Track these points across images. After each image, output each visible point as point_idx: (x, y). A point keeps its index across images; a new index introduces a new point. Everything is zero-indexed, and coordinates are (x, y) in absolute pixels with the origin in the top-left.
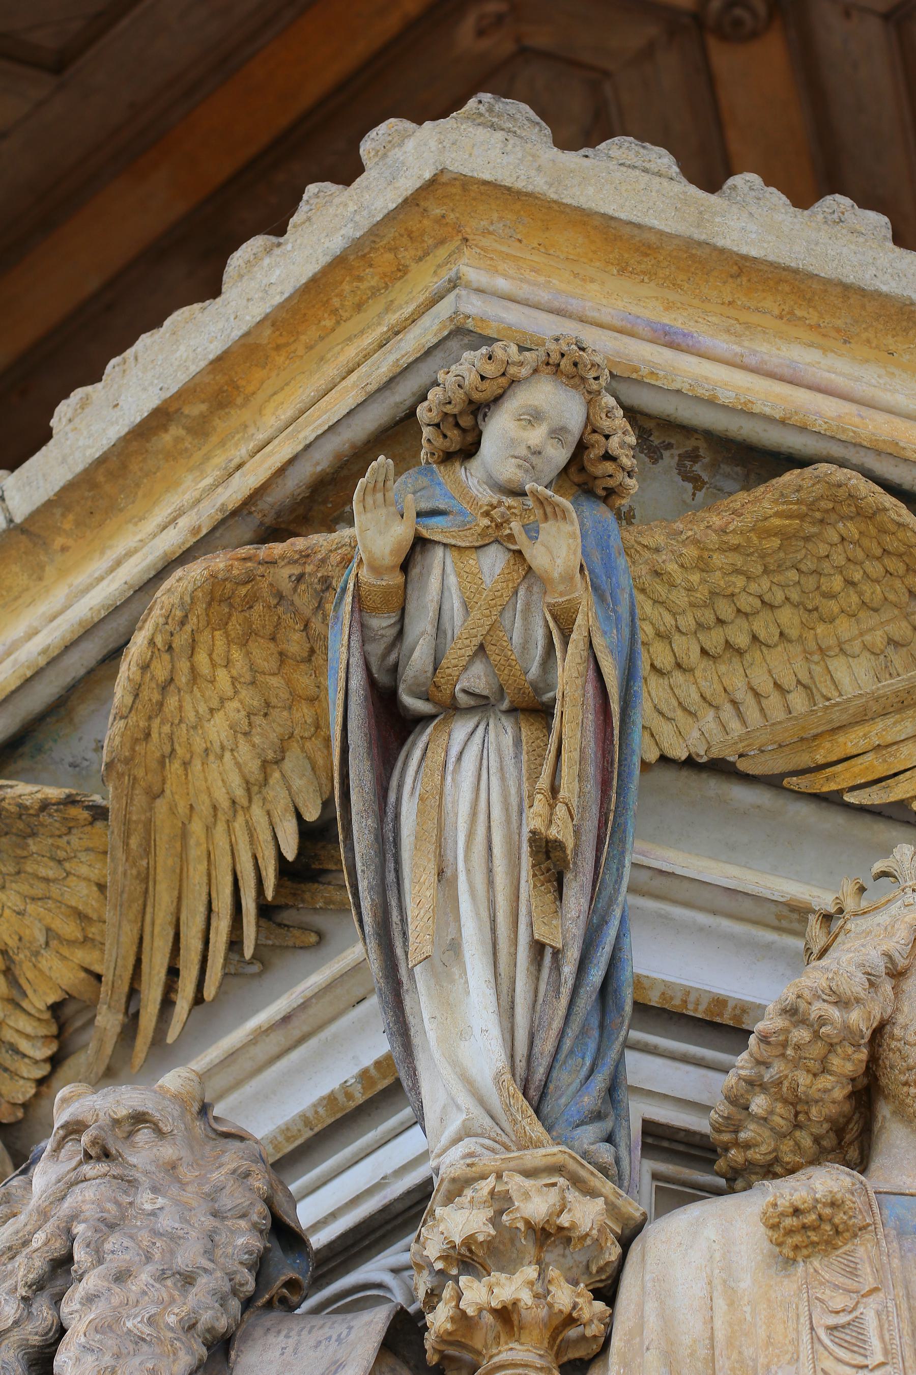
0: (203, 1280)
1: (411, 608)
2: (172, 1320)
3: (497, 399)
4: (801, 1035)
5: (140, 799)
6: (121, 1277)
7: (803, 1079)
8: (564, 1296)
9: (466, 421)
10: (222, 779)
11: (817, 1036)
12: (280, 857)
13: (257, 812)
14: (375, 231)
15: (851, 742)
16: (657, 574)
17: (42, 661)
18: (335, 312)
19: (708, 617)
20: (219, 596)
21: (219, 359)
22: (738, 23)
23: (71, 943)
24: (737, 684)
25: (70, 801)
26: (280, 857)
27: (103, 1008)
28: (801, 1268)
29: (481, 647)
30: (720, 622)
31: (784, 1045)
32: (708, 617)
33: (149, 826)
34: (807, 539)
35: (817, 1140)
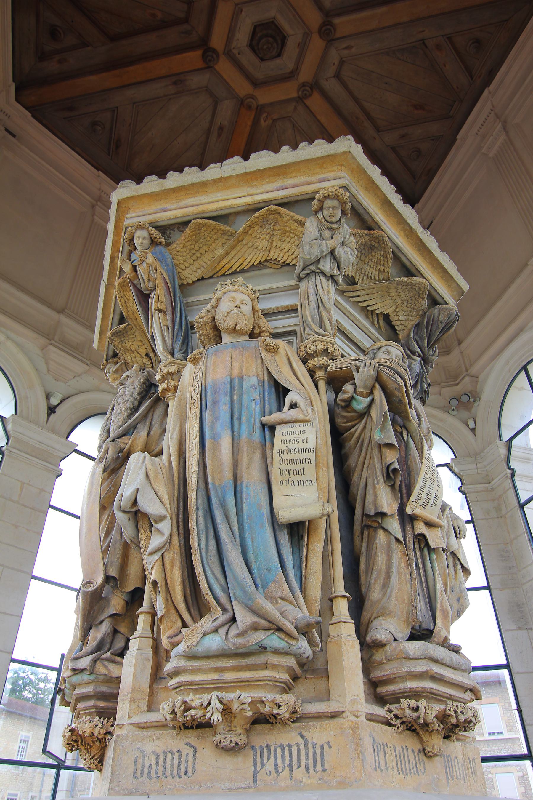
0: (130, 400)
2: (124, 409)
3: (133, 237)
5: (134, 321)
6: (119, 405)
7: (205, 332)
8: (172, 383)
9: (132, 243)
15: (222, 264)
16: (178, 252)
19: (191, 254)
22: (306, 94)
24: (202, 263)
25: (128, 325)
30: (194, 254)
32: (191, 254)
33: (138, 324)
34: (199, 233)
35: (214, 340)
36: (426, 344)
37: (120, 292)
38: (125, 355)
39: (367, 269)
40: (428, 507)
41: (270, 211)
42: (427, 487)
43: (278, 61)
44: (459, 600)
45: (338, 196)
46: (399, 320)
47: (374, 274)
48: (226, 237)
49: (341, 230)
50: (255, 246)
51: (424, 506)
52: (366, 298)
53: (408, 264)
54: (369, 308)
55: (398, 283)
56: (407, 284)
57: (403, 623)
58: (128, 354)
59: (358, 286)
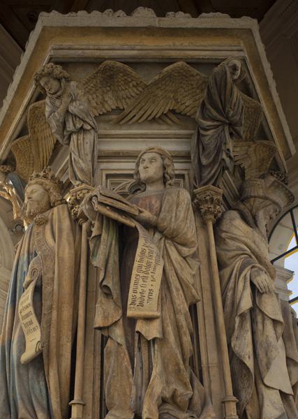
36: (215, 113)
39: (121, 94)
40: (145, 304)
42: (139, 287)
44: (267, 355)
45: (41, 74)
46: (187, 107)
47: (133, 91)
49: (69, 90)
51: (141, 304)
52: (141, 112)
53: (157, 61)
54: (150, 118)
55: (156, 83)
56: (163, 79)
57: (128, 411)
59: (126, 111)
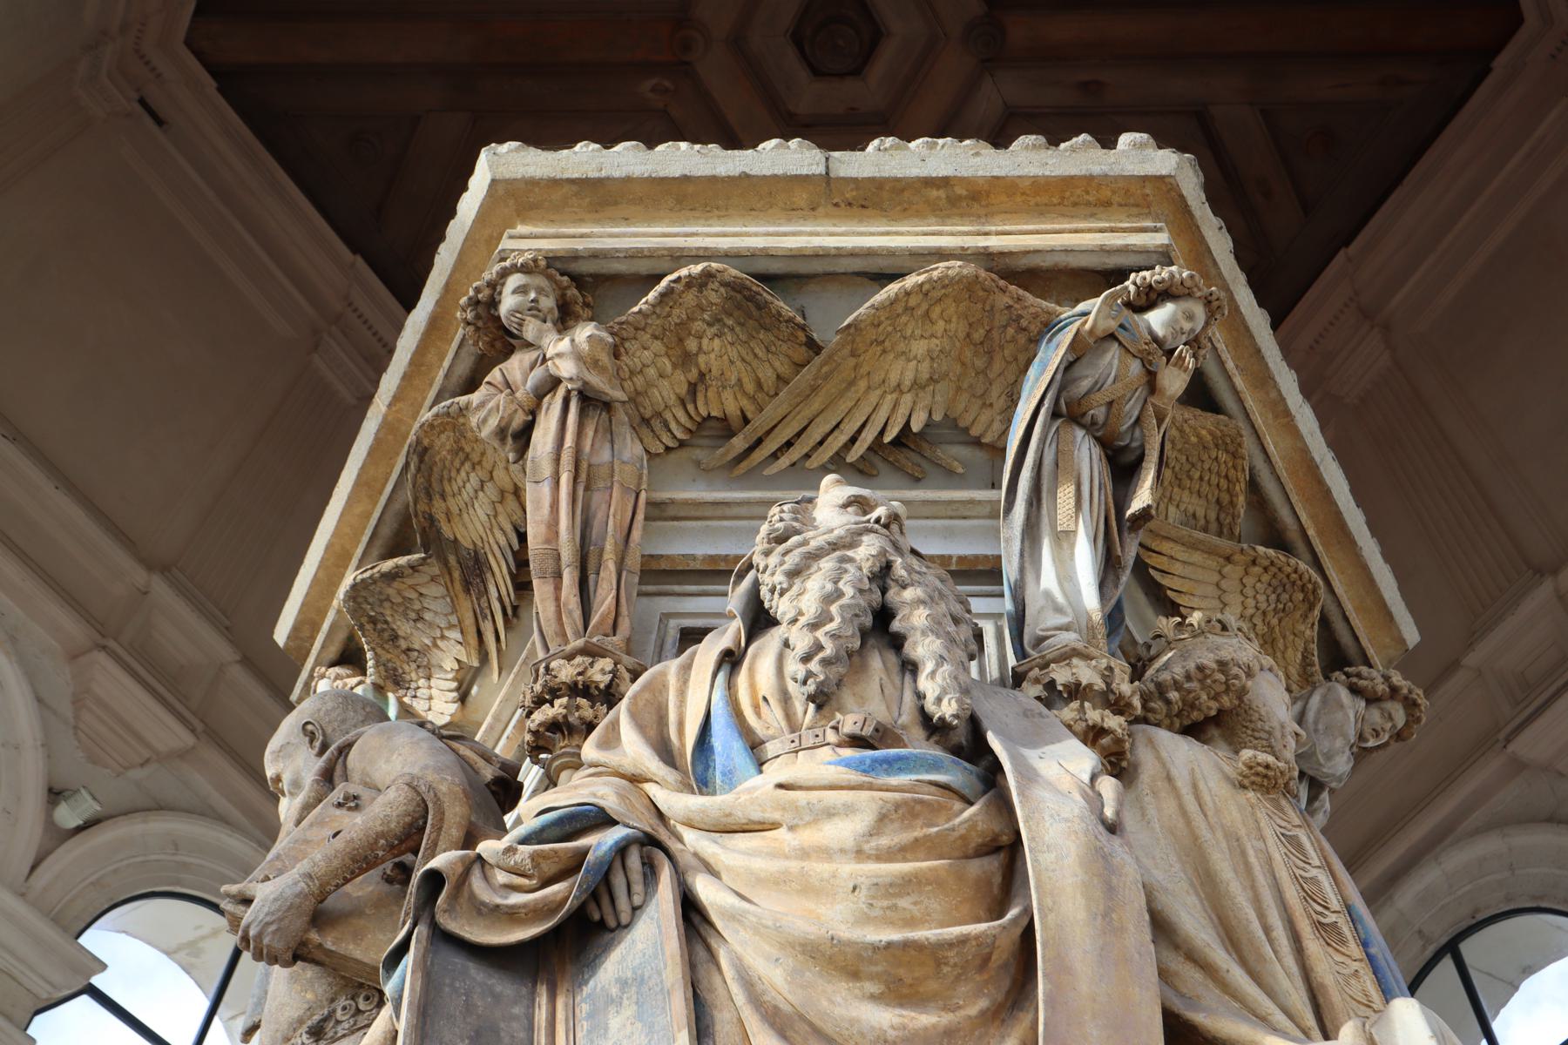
1: (1084, 361)
4: (1221, 677)
9: (1153, 296)
10: (901, 371)
11: (1226, 683)
12: (907, 424)
13: (907, 399)
14: (1117, 178)
15: (1166, 547)
17: (833, 252)
18: (1063, 198)
20: (969, 287)
21: (997, 178)
23: (745, 393)
25: (803, 328)
26: (907, 424)
27: (741, 436)
28: (1251, 794)
29: (1110, 404)
31: (1206, 677)
37: (944, 287)
38: (645, 337)
41: (1314, 591)
43: (803, 74)
48: (1212, 515)
50: (1226, 598)
58: (657, 346)
